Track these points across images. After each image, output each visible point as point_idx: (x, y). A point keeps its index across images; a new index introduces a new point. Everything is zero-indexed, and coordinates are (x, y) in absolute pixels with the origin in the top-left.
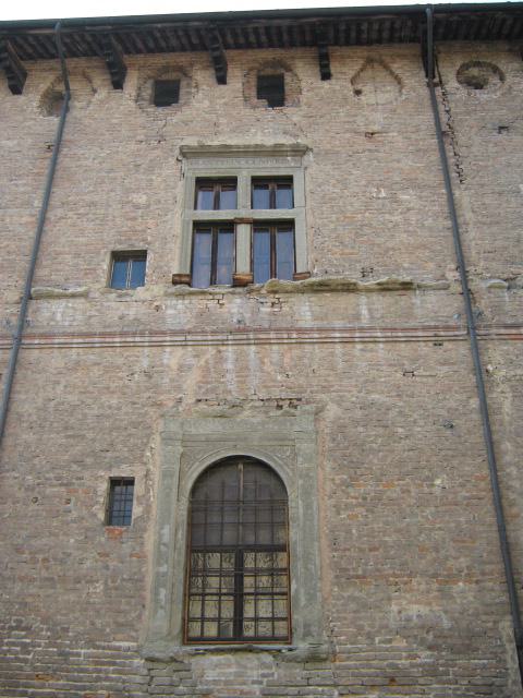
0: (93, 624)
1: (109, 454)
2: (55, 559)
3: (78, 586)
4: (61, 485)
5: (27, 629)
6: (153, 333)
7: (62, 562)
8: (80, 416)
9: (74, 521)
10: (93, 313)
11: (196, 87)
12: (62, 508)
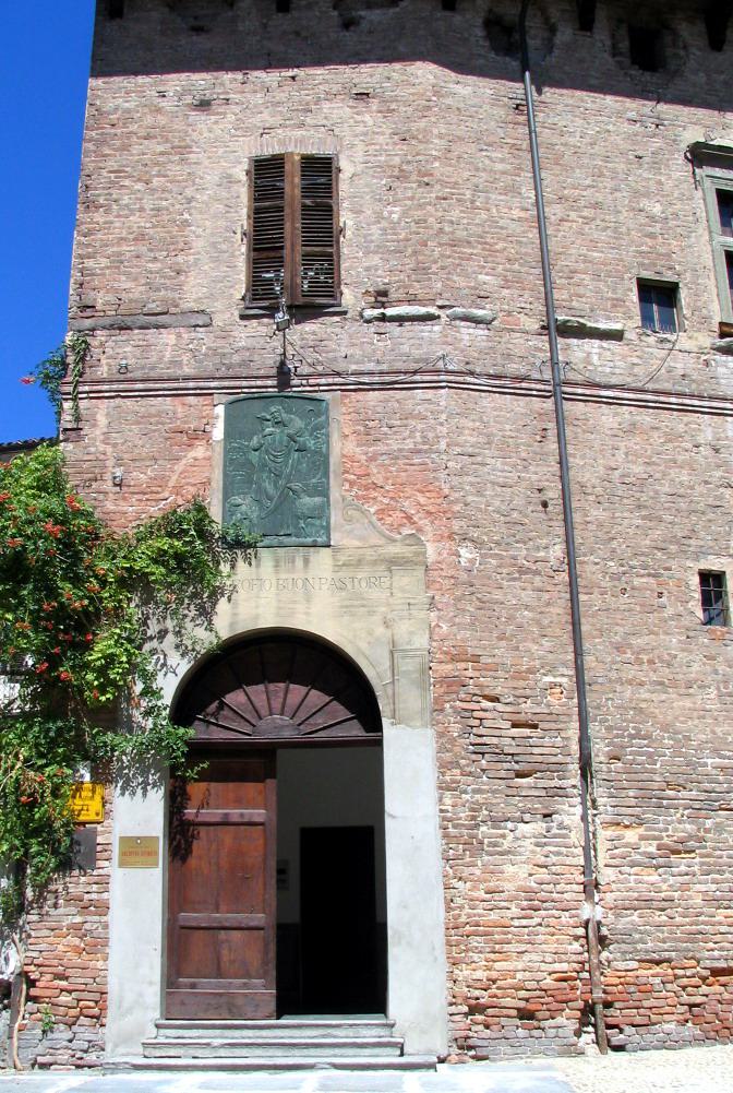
0: (713, 732)
1: (692, 542)
2: (662, 661)
3: (691, 691)
4: (649, 575)
6: (711, 398)
7: (669, 665)
8: (651, 494)
9: (672, 619)
10: (636, 361)
11: (685, 47)
12: (657, 601)
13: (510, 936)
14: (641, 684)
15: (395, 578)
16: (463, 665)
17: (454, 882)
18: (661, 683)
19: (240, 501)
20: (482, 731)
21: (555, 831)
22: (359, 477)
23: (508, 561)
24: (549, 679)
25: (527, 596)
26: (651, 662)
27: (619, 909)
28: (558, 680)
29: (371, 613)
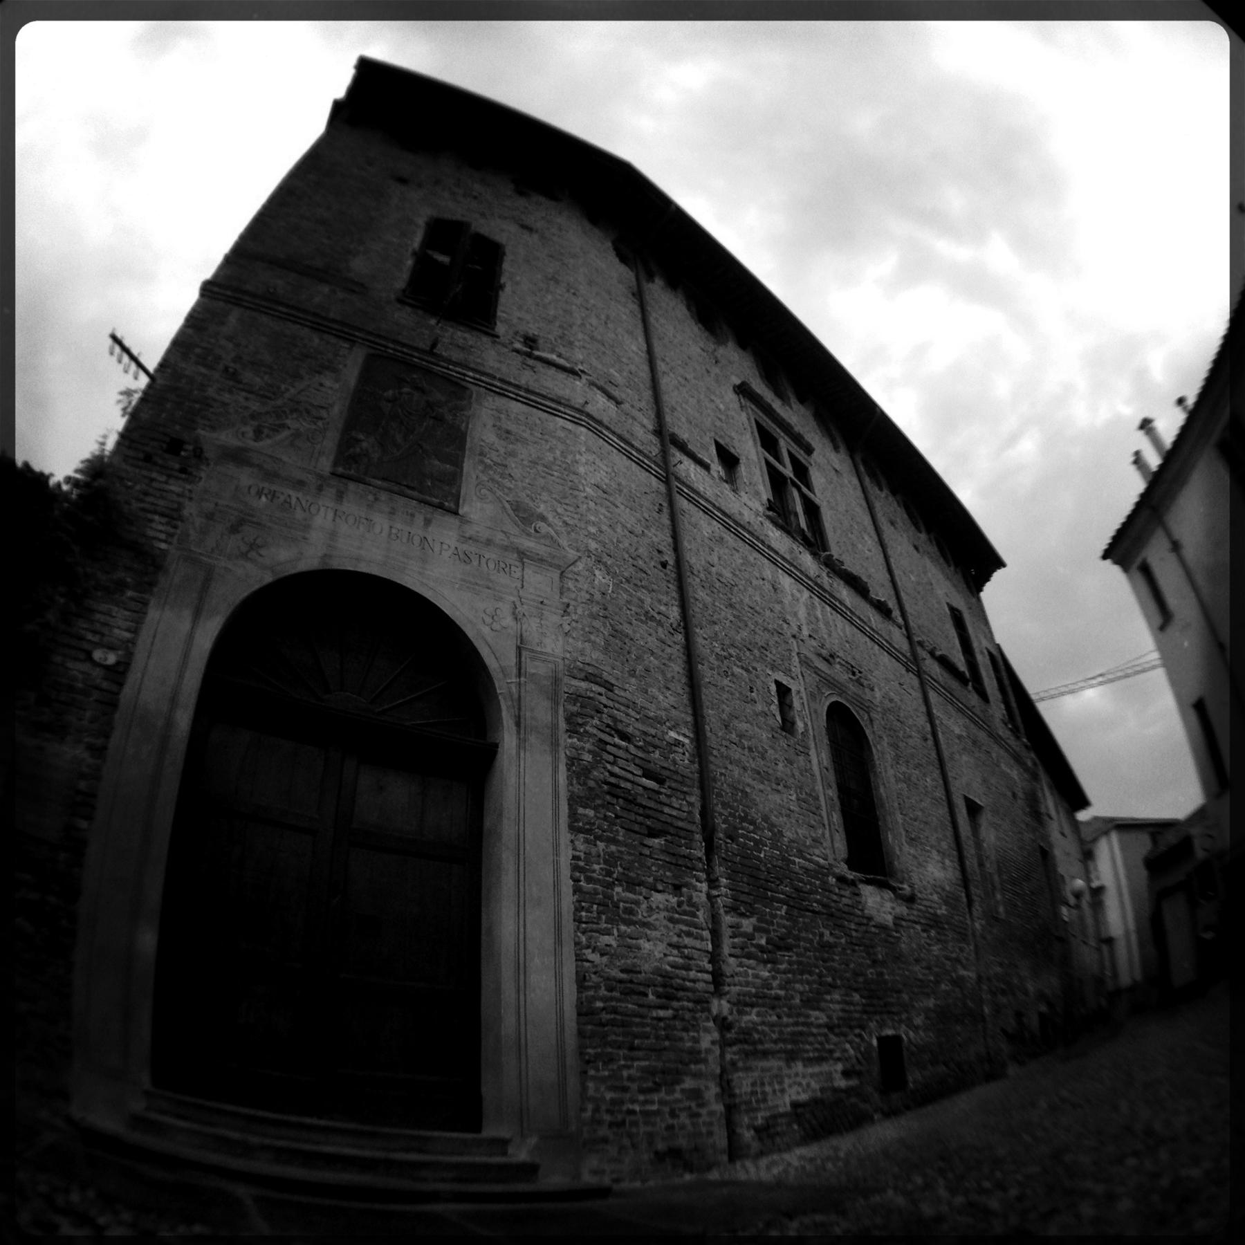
5: (752, 822)
13: (648, 1029)
14: (745, 769)
15: (526, 570)
16: (596, 688)
17: (589, 954)
18: (759, 773)
19: (361, 437)
20: (616, 770)
21: (685, 907)
22: (496, 464)
23: (635, 600)
24: (672, 734)
25: (652, 642)
26: (750, 749)
27: (742, 1004)
28: (681, 738)
29: (500, 599)
